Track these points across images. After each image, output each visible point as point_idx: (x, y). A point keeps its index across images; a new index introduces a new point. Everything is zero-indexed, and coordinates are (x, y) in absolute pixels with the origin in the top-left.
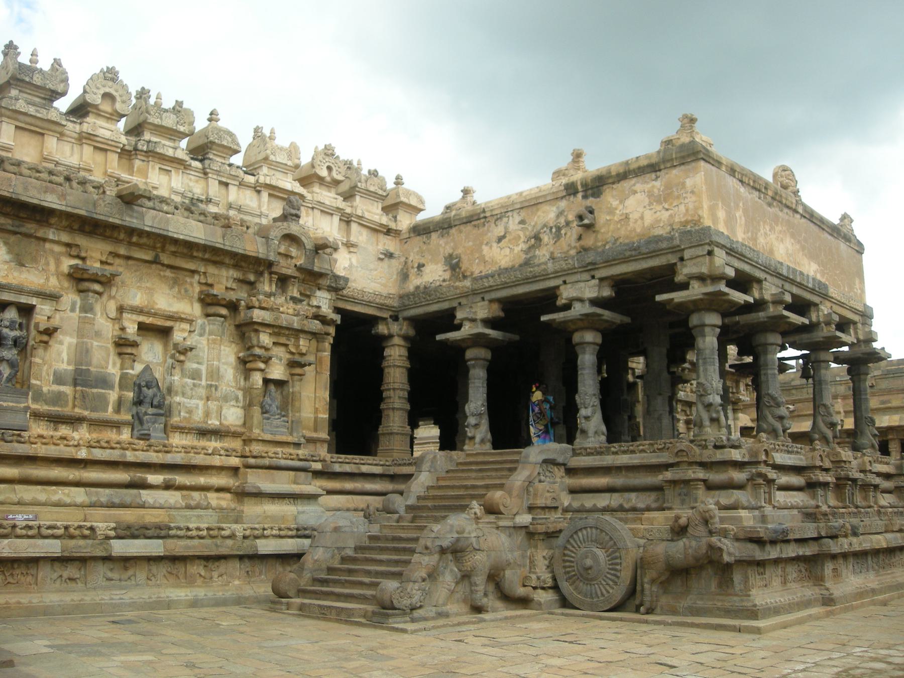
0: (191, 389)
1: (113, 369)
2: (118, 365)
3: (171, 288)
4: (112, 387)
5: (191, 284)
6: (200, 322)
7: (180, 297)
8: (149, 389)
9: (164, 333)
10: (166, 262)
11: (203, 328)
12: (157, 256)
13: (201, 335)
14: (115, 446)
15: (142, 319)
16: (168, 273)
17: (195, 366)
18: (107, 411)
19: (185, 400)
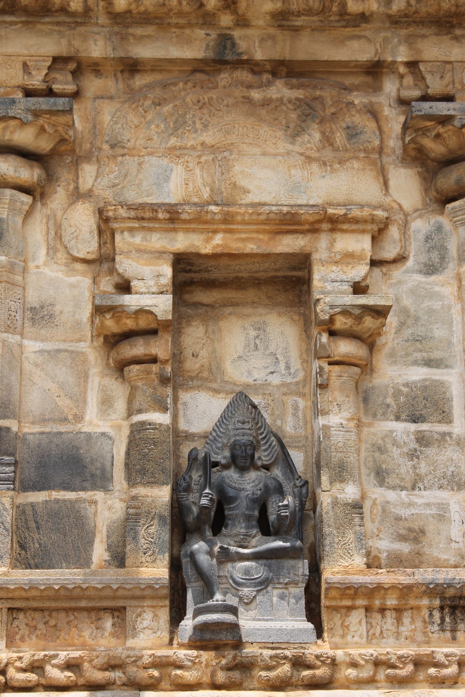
0: (413, 455)
1: (103, 417)
2: (121, 406)
3: (295, 133)
4: (101, 480)
5: (373, 113)
6: (420, 226)
7: (332, 156)
8: (243, 470)
9: (288, 283)
10: (259, 56)
11: (435, 243)
12: (225, 41)
13: (430, 269)
14: (99, 676)
15: (182, 242)
16: (279, 90)
17: (418, 374)
18: (86, 562)
19: (391, 495)
